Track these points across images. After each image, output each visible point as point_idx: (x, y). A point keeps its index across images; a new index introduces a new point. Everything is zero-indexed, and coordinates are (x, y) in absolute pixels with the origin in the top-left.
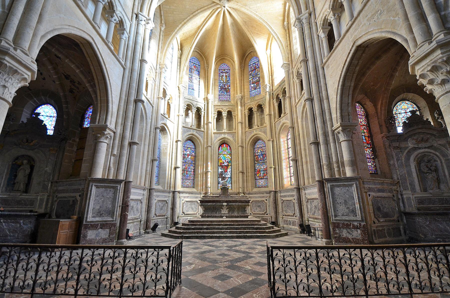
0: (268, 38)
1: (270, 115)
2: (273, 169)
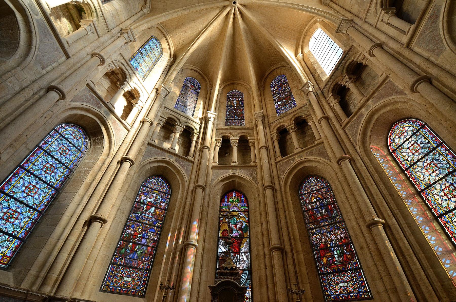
0: (297, 44)
2: (381, 227)
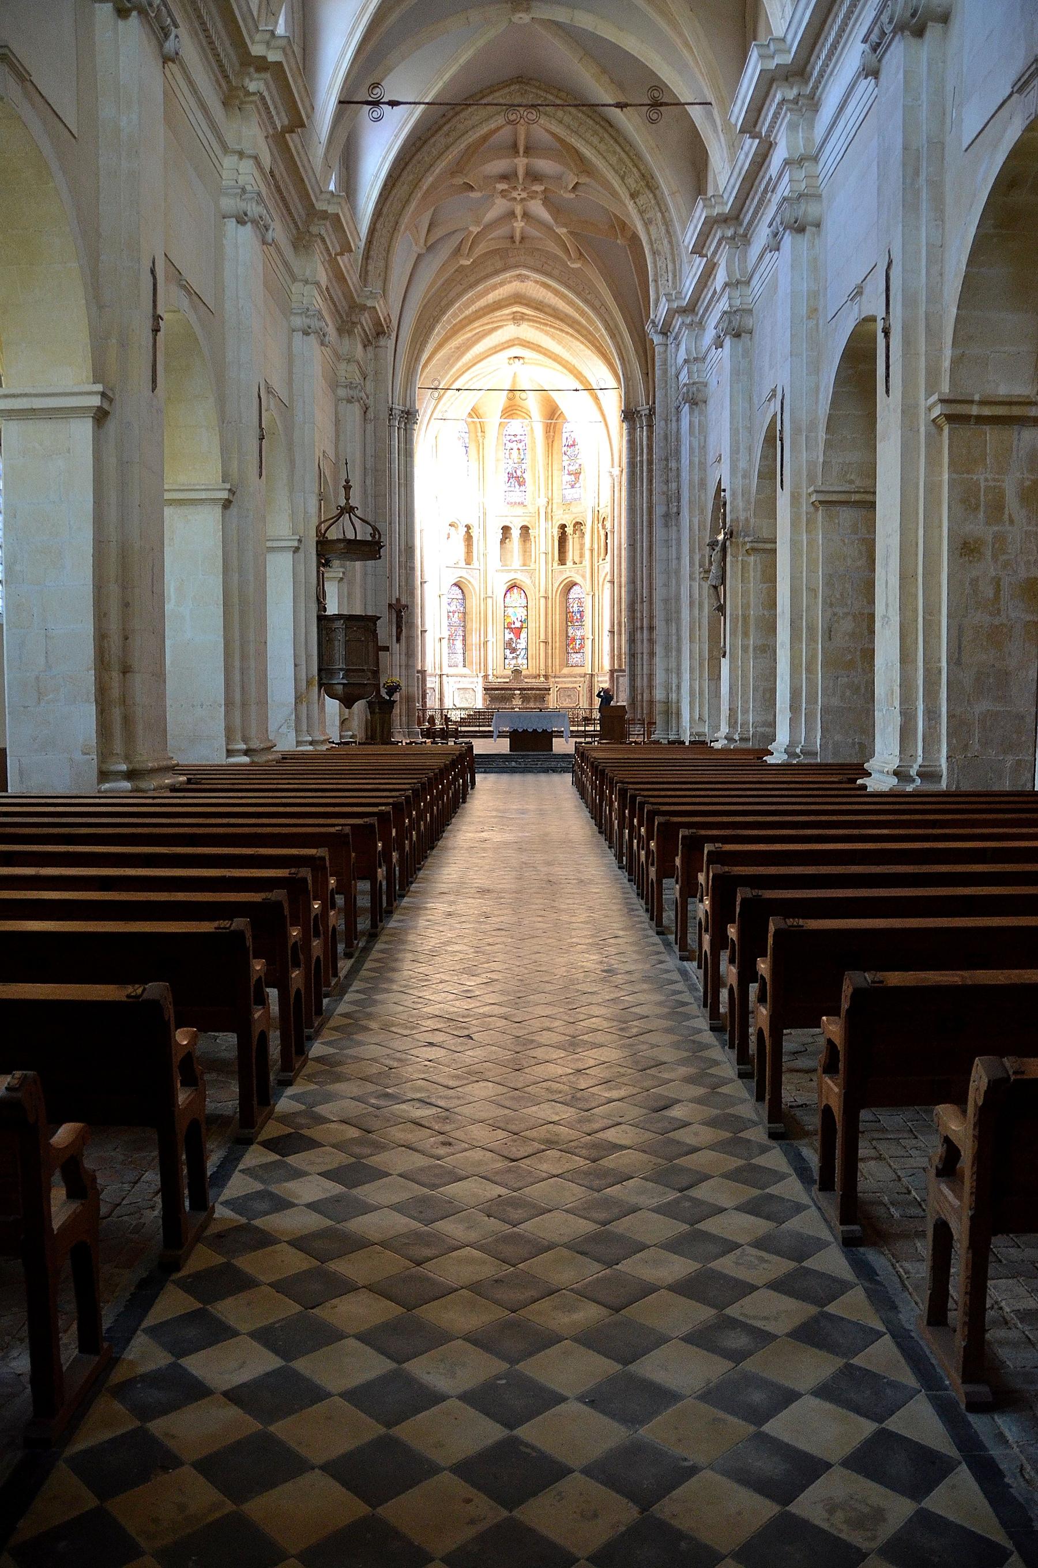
1: (592, 550)
